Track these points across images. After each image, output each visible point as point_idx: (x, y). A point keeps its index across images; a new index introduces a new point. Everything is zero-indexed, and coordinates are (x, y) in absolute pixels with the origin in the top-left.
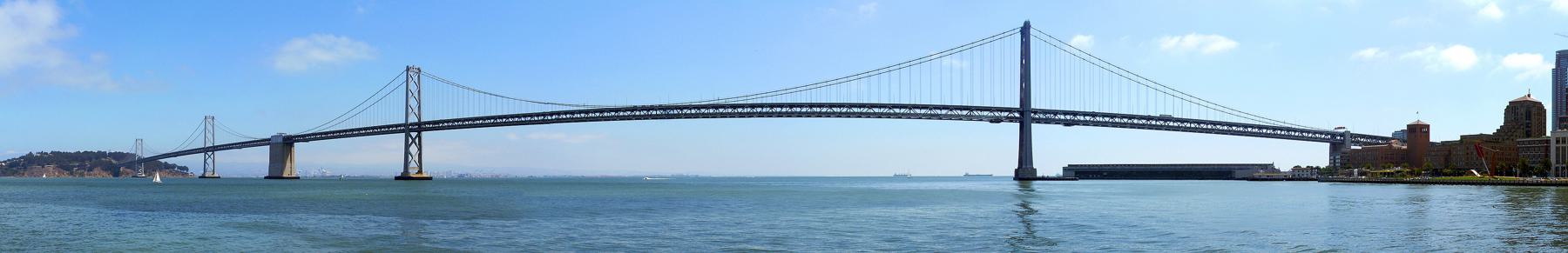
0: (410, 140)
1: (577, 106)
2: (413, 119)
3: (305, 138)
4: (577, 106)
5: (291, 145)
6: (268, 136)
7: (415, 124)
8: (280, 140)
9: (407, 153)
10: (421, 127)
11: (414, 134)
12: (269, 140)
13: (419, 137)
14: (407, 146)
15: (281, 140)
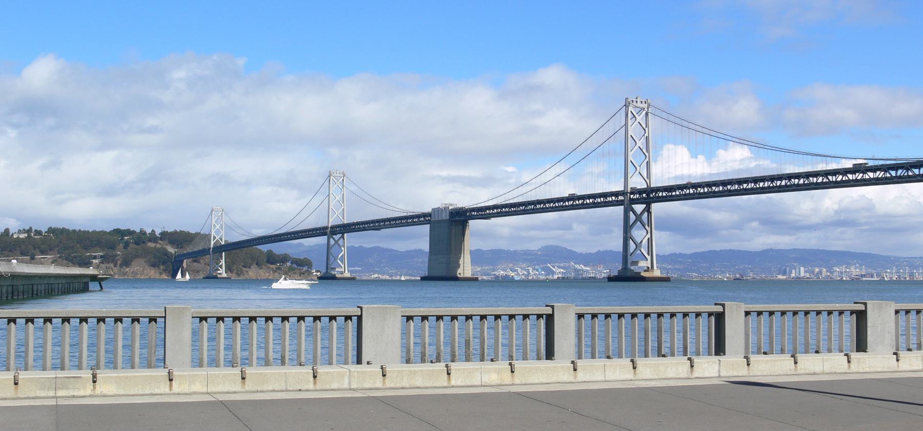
0: (632, 217)
1: (895, 160)
2: (637, 182)
3: (483, 213)
4: (895, 160)
5: (464, 225)
6: (427, 209)
7: (640, 192)
8: (446, 216)
9: (627, 237)
10: (650, 196)
11: (639, 208)
12: (429, 215)
13: (648, 210)
14: (627, 228)
15: (448, 218)
